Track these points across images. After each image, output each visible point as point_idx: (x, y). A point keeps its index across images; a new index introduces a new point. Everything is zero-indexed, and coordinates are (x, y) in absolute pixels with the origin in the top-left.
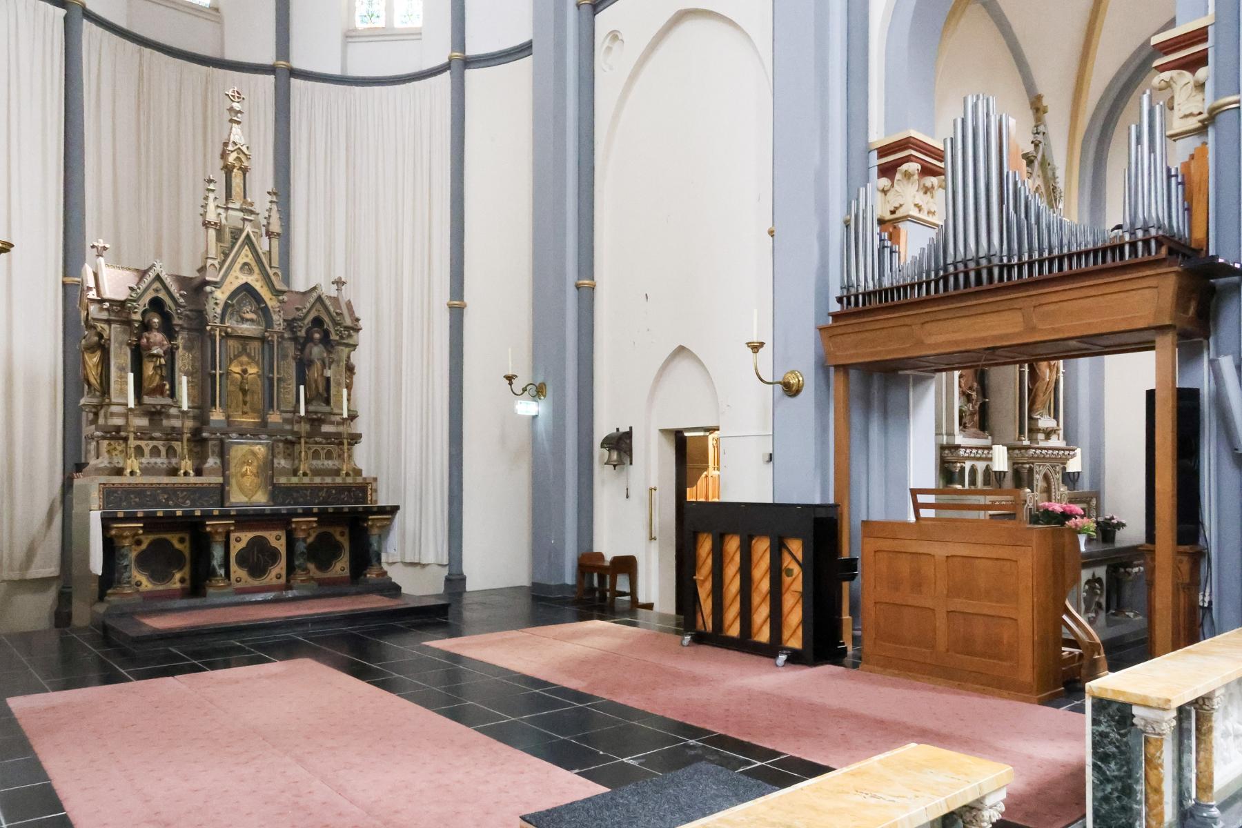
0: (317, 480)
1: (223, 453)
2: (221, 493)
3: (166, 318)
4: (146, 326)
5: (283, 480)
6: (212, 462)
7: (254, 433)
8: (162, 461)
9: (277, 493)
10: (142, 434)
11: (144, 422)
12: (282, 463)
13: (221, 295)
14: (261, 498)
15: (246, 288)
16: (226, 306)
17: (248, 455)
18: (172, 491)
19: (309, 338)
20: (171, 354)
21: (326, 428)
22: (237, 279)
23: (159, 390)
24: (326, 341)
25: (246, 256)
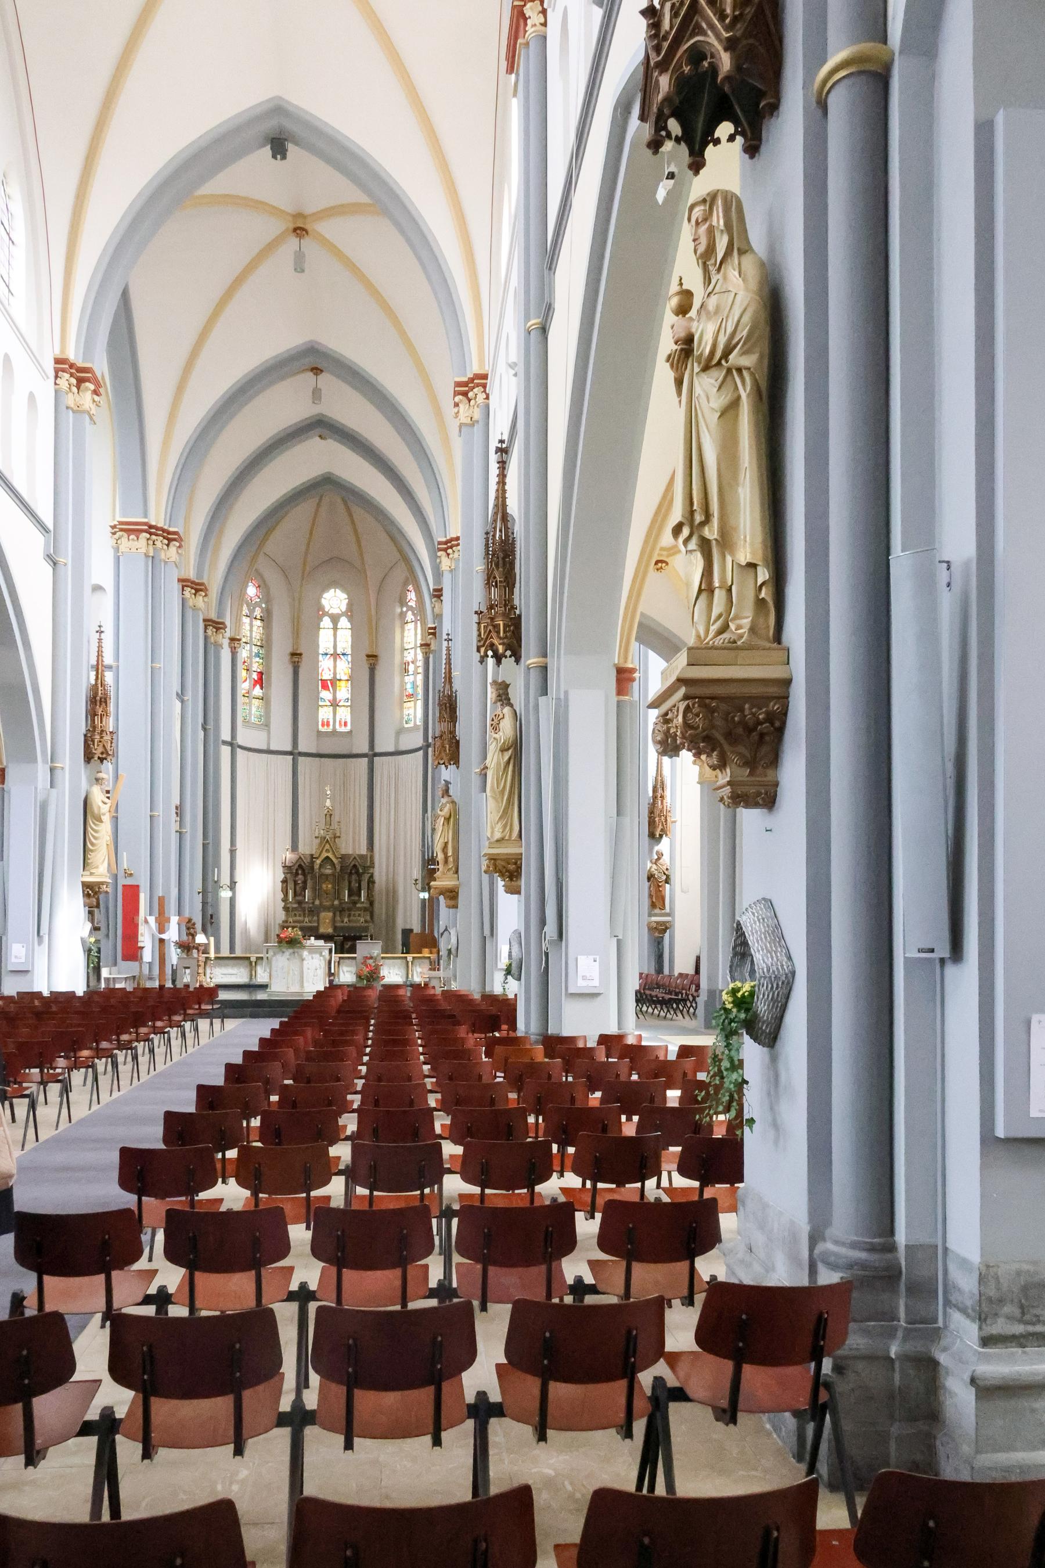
0: (351, 925)
2: (317, 928)
3: (303, 870)
4: (297, 874)
5: (338, 924)
6: (315, 918)
7: (327, 909)
8: (301, 918)
9: (335, 928)
10: (294, 909)
11: (295, 906)
12: (338, 918)
13: (318, 862)
14: (330, 930)
15: (327, 857)
16: (321, 866)
17: (326, 916)
19: (351, 873)
20: (305, 882)
21: (358, 905)
22: (325, 855)
23: (300, 895)
24: (357, 872)
25: (327, 847)
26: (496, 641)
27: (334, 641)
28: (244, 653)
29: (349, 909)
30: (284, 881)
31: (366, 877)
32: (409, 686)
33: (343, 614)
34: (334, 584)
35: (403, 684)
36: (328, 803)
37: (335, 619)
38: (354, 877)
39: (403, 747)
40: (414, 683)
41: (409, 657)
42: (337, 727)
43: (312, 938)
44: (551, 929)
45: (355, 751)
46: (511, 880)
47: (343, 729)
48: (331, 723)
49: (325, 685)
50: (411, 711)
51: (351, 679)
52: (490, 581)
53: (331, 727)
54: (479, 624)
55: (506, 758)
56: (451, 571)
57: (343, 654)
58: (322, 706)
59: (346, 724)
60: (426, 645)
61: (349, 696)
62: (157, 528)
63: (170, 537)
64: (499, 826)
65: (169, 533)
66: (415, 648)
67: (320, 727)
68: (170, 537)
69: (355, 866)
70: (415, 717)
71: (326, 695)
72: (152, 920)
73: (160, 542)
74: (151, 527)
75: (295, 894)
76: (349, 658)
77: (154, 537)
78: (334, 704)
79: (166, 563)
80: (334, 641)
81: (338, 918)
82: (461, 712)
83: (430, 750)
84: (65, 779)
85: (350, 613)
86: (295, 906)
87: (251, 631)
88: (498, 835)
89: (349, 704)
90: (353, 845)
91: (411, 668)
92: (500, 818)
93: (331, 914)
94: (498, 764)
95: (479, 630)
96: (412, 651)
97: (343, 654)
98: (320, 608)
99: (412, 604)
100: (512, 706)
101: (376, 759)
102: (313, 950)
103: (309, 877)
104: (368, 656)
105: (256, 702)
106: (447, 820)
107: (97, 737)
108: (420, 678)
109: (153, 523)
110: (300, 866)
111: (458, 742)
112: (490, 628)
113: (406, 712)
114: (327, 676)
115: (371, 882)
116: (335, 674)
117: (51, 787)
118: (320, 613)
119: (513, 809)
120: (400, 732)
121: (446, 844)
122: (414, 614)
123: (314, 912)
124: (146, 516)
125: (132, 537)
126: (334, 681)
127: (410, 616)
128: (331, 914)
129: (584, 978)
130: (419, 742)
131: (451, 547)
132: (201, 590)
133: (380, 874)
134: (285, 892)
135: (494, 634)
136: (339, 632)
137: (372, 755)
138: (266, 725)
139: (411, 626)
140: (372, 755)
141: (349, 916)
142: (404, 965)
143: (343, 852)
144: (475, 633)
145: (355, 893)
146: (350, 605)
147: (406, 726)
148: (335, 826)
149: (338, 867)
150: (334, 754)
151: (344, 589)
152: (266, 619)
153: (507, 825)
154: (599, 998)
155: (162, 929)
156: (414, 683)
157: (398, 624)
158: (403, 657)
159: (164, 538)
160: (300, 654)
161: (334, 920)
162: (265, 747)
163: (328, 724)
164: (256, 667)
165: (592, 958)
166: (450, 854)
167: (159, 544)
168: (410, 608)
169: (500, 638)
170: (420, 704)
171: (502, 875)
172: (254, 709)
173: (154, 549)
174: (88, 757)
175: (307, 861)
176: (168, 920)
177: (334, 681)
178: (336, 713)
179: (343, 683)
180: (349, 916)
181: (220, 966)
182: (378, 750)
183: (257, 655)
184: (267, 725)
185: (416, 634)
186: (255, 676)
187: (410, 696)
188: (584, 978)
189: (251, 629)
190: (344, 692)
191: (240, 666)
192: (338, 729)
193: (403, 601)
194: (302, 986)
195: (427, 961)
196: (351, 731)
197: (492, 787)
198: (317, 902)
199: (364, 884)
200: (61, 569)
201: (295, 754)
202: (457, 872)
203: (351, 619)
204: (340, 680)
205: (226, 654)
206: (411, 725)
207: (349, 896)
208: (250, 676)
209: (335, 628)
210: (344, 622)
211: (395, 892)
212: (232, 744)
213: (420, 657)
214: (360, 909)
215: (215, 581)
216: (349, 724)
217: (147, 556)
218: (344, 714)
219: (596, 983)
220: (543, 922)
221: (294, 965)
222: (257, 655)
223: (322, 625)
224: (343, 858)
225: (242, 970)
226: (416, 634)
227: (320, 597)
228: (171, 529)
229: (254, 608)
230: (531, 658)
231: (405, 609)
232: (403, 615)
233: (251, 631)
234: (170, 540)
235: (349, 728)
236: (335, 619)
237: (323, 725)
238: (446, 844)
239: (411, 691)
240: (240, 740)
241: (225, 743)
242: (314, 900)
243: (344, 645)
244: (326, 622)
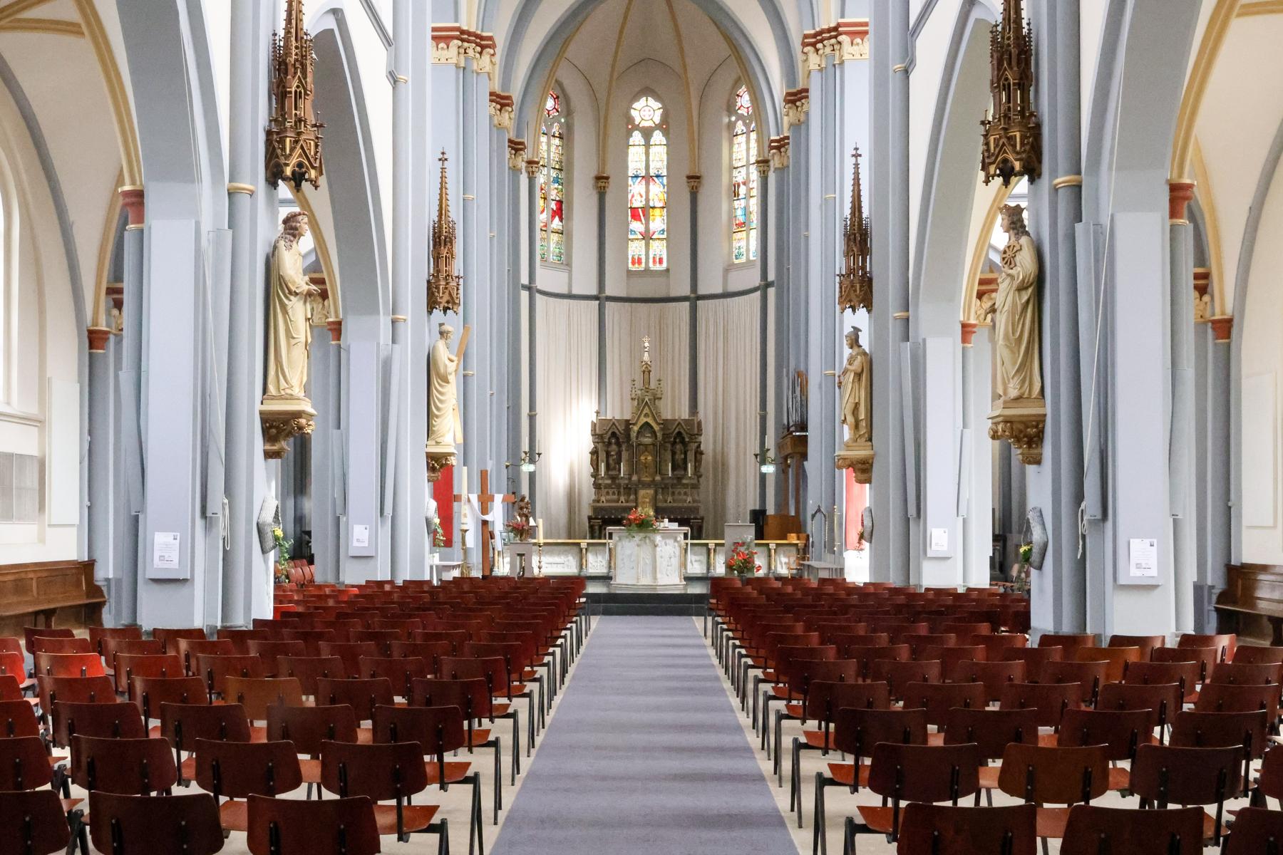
1: (636, 494)
4: (610, 443)
5: (660, 504)
6: (632, 497)
8: (615, 497)
10: (607, 486)
11: (609, 482)
13: (636, 428)
15: (647, 424)
18: (616, 509)
20: (619, 454)
21: (684, 481)
22: (643, 420)
24: (683, 442)
26: (1011, 157)
27: (647, 159)
28: (541, 179)
29: (673, 486)
30: (594, 453)
31: (694, 446)
32: (739, 212)
33: (658, 127)
34: (647, 91)
35: (732, 210)
36: (646, 357)
37: (647, 133)
38: (678, 447)
39: (732, 288)
40: (746, 209)
41: (739, 177)
42: (651, 264)
43: (666, 520)
44: (1091, 504)
45: (673, 294)
46: (1030, 447)
47: (658, 267)
50: (743, 243)
52: (1000, 84)
54: (986, 136)
55: (1025, 298)
56: (821, 70)
57: (657, 176)
58: (632, 240)
59: (661, 261)
60: (763, 163)
61: (665, 227)
62: (469, 33)
63: (483, 43)
64: (1017, 380)
65: (482, 38)
66: (747, 165)
68: (483, 43)
69: (679, 433)
70: (748, 250)
71: (637, 226)
72: (474, 498)
73: (472, 49)
74: (463, 32)
75: (608, 467)
77: (466, 44)
78: (647, 237)
79: (478, 74)
80: (647, 159)
81: (660, 497)
82: (875, 243)
83: (771, 292)
84: (407, 332)
86: (609, 482)
87: (549, 151)
88: (1013, 393)
90: (675, 408)
91: (742, 190)
92: (1018, 371)
93: (651, 492)
94: (1014, 304)
95: (987, 144)
96: (744, 170)
97: (657, 176)
98: (630, 120)
99: (743, 112)
100: (1027, 234)
101: (699, 303)
102: (667, 534)
103: (624, 448)
104: (689, 177)
105: (555, 237)
106: (858, 375)
107: (443, 283)
108: (754, 205)
109: (465, 28)
110: (614, 434)
111: (870, 280)
112: (1004, 140)
113: (736, 244)
114: (638, 203)
115: (699, 453)
116: (647, 200)
117: (394, 341)
118: (630, 125)
119: (1032, 362)
120: (729, 268)
121: (857, 406)
122: (745, 124)
123: (631, 489)
124: (456, 21)
125: (442, 45)
126: (647, 209)
127: (740, 127)
128: (651, 492)
129: (1138, 566)
130: (756, 281)
131: (821, 41)
132: (508, 105)
133: (707, 442)
134: (595, 464)
135: (1008, 149)
136: (652, 150)
137: (694, 299)
138: (565, 262)
139: (742, 139)
140: (694, 299)
141: (673, 493)
142: (766, 553)
143: (664, 417)
144: (981, 148)
145: (679, 466)
147: (736, 262)
148: (653, 386)
149: (659, 435)
150: (648, 298)
151: (657, 98)
153: (1026, 380)
154: (1157, 591)
155: (484, 510)
156: (746, 209)
157: (725, 134)
158: (731, 177)
159: (477, 44)
160: (607, 178)
161: (655, 499)
162: (564, 291)
163: (640, 262)
164: (554, 195)
165: (1147, 541)
166: (862, 416)
167: (471, 52)
168: (741, 117)
169: (1018, 153)
170: (754, 235)
171: (1018, 440)
172: (552, 246)
173: (466, 59)
174: (432, 304)
175: (621, 428)
176: (492, 499)
177: (647, 209)
178: (649, 247)
179: (657, 212)
180: (673, 493)
181: (551, 553)
182: (702, 291)
183: (556, 180)
184: (569, 265)
185: (748, 149)
186: (553, 206)
187: (741, 225)
188: (1138, 566)
189: (548, 149)
190: (658, 222)
191: (538, 194)
193: (731, 108)
194: (655, 578)
195: (794, 550)
196: (667, 270)
197: (1006, 335)
198: (635, 478)
199: (691, 456)
200: (401, 85)
201: (601, 298)
202: (870, 440)
203: (666, 133)
204: (654, 208)
205: (524, 179)
206: (743, 259)
207: (673, 469)
209: (647, 145)
210: (658, 137)
211: (724, 465)
212: (529, 288)
213: (754, 174)
214: (686, 486)
215: (516, 92)
217: (457, 67)
218: (659, 248)
219: (1154, 572)
220: (1079, 497)
221: (644, 553)
222: (556, 180)
224: (665, 424)
225: (571, 558)
226: (748, 149)
227: (630, 107)
228: (485, 34)
229: (552, 125)
230: (1056, 175)
231: (733, 119)
232: (731, 126)
233: (549, 151)
234: (483, 47)
235: (665, 265)
236: (647, 133)
237: (633, 263)
238: (857, 406)
239: (741, 219)
240: (540, 284)
241: (524, 287)
242: (630, 475)
243: (659, 165)
244: (637, 137)
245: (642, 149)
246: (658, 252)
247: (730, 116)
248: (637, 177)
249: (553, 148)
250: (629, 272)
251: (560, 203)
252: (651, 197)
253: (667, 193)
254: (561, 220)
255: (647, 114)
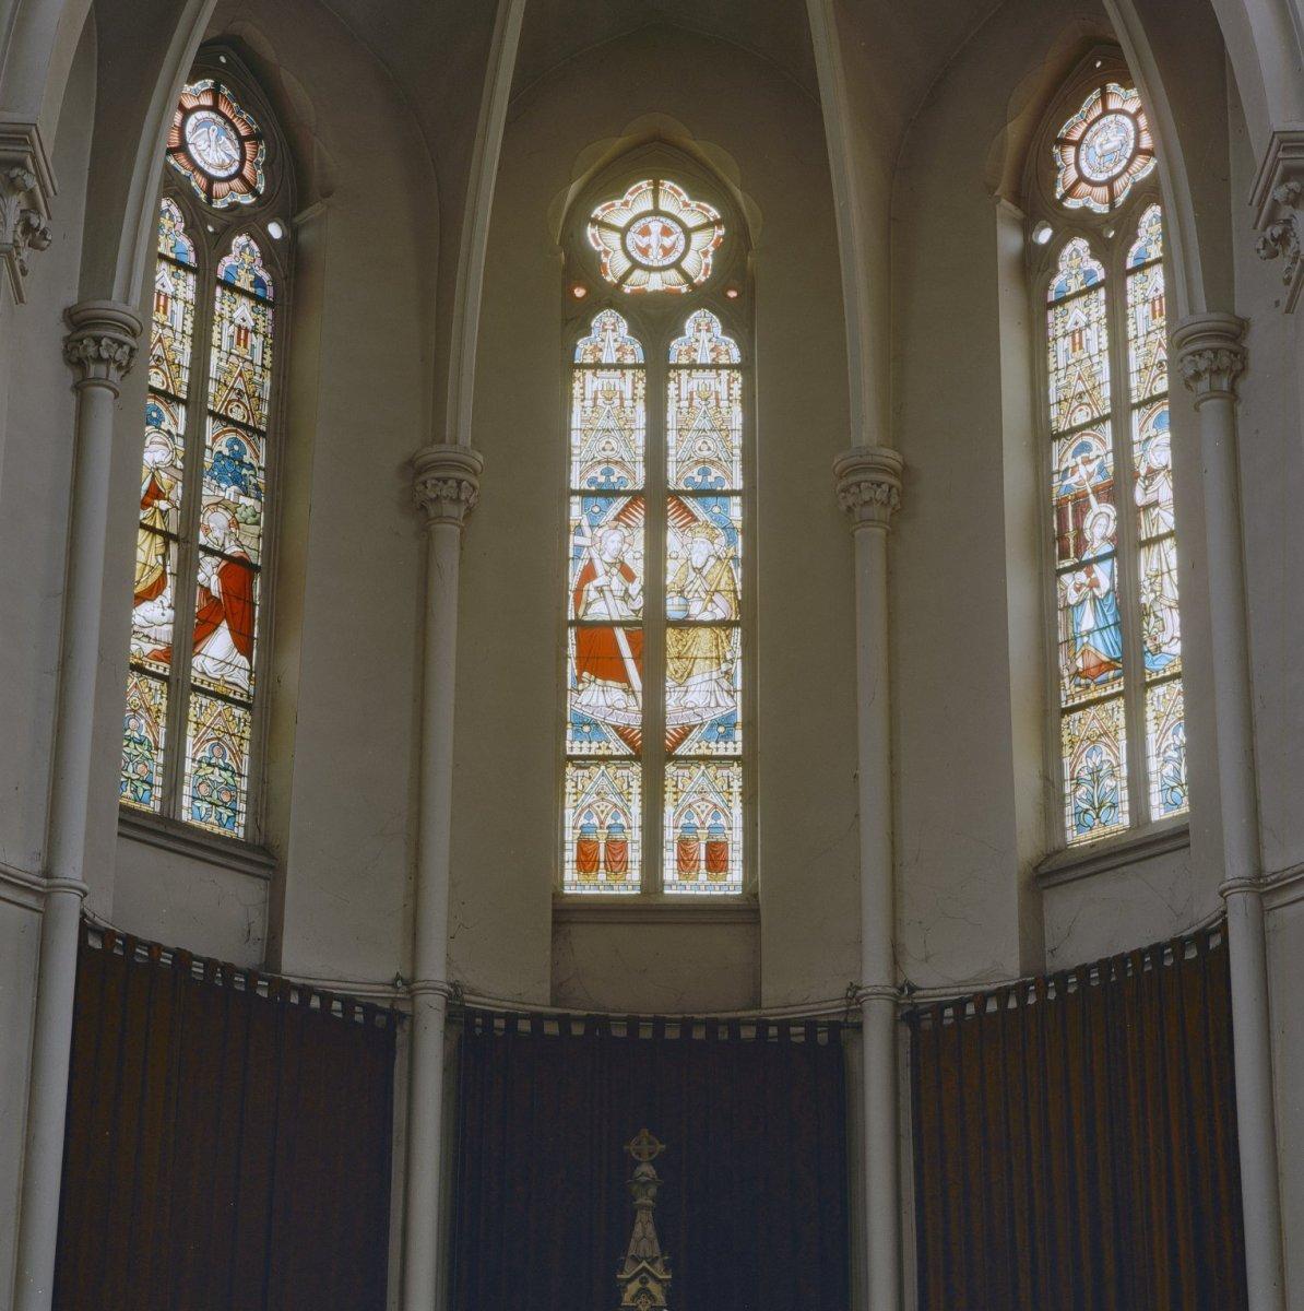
34: (655, 157)
42: (670, 872)
47: (702, 885)
48: (635, 854)
49: (600, 661)
51: (750, 616)
53: (635, 875)
58: (583, 761)
61: (733, 705)
66: (1121, 411)
67: (570, 873)
71: (602, 703)
76: (735, 511)
85: (735, 291)
89: (735, 747)
91: (1100, 523)
96: (1101, 444)
98: (584, 265)
113: (1077, 763)
116: (655, 589)
122: (1100, 249)
126: (653, 631)
136: (681, 387)
146: (731, 259)
151: (702, 183)
152: (289, 291)
163: (617, 860)
164: (228, 522)
183: (233, 468)
192: (678, 884)
204: (685, 624)
208: (187, 568)
209: (657, 371)
210: (703, 336)
216: (736, 856)
218: (710, 804)
223: (583, 350)
231: (1044, 236)
232: (1036, 266)
235: (733, 879)
236: (656, 320)
237: (586, 862)
243: (708, 447)
244: (610, 336)
245: (630, 386)
246: (702, 817)
247: (1027, 227)
248: (610, 494)
249: (222, 335)
250: (569, 915)
251: (237, 569)
252: (673, 573)
253: (748, 563)
254: (243, 644)
255: (654, 241)
